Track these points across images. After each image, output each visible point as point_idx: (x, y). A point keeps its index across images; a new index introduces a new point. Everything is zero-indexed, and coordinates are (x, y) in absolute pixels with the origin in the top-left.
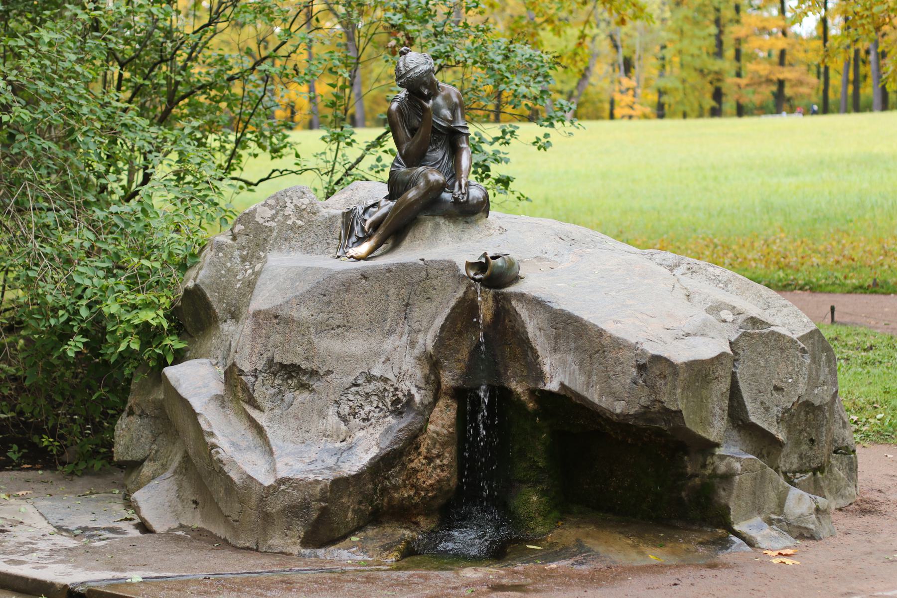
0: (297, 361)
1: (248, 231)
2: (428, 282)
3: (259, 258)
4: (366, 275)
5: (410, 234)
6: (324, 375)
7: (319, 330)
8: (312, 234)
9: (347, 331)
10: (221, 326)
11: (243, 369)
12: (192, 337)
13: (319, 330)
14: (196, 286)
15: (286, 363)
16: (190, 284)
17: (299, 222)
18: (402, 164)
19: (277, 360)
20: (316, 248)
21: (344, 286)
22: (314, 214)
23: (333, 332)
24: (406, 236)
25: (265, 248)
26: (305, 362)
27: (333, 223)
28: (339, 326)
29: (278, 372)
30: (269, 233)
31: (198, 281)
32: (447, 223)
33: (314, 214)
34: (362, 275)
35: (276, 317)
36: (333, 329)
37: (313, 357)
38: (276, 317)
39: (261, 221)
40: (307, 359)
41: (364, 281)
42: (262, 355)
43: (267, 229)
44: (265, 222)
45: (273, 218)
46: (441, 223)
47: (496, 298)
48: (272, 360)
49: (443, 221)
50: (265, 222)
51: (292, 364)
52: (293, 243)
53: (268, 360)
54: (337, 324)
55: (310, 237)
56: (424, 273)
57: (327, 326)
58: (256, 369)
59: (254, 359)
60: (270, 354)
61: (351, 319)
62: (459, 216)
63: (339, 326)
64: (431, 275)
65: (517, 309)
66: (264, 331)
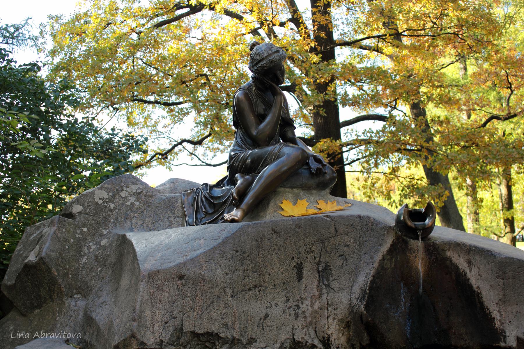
0: (214, 328)
1: (88, 210)
2: (338, 238)
3: (102, 235)
4: (277, 230)
5: (272, 204)
6: (247, 344)
7: (236, 290)
8: (152, 214)
9: (264, 291)
10: (67, 302)
11: (145, 341)
12: (23, 315)
13: (236, 290)
14: (42, 261)
15: (199, 332)
16: (32, 258)
17: (137, 203)
18: (244, 148)
19: (187, 328)
20: (158, 225)
21: (257, 241)
22: (151, 196)
23: (250, 293)
24: (268, 207)
25: (107, 225)
26: (225, 330)
27: (173, 203)
28: (255, 286)
29: (188, 343)
30: (109, 213)
31: (43, 254)
32: (305, 194)
33: (151, 196)
34: (273, 230)
35: (181, 277)
36: (250, 290)
37: (233, 323)
38: (181, 277)
39: (100, 202)
40: (226, 325)
41: (275, 236)
42: (166, 323)
43: (107, 209)
44: (104, 202)
45: (112, 199)
46: (301, 194)
47: (428, 250)
48: (182, 329)
49: (302, 193)
50: (104, 202)
51: (208, 333)
52: (134, 221)
53: (176, 329)
54: (254, 284)
55: (150, 216)
56: (333, 229)
57: (244, 286)
58: (162, 341)
59: (156, 328)
60: (177, 322)
61: (266, 278)
62: (315, 189)
63: (255, 286)
64: (340, 231)
65: (454, 260)
66: (167, 295)
